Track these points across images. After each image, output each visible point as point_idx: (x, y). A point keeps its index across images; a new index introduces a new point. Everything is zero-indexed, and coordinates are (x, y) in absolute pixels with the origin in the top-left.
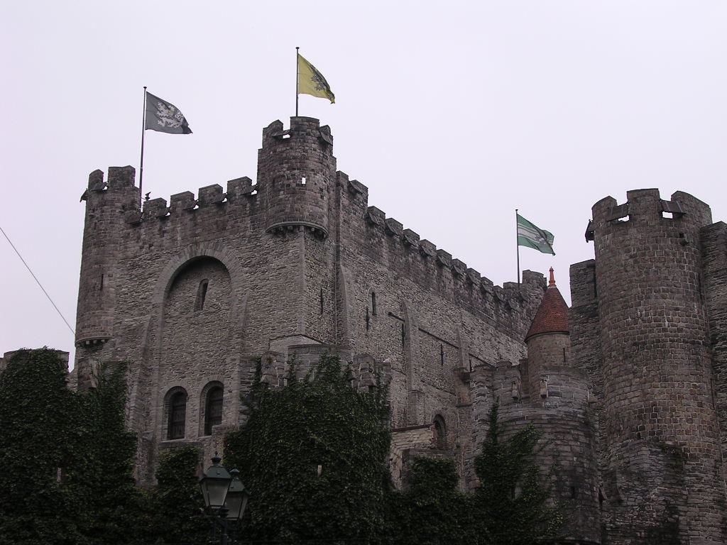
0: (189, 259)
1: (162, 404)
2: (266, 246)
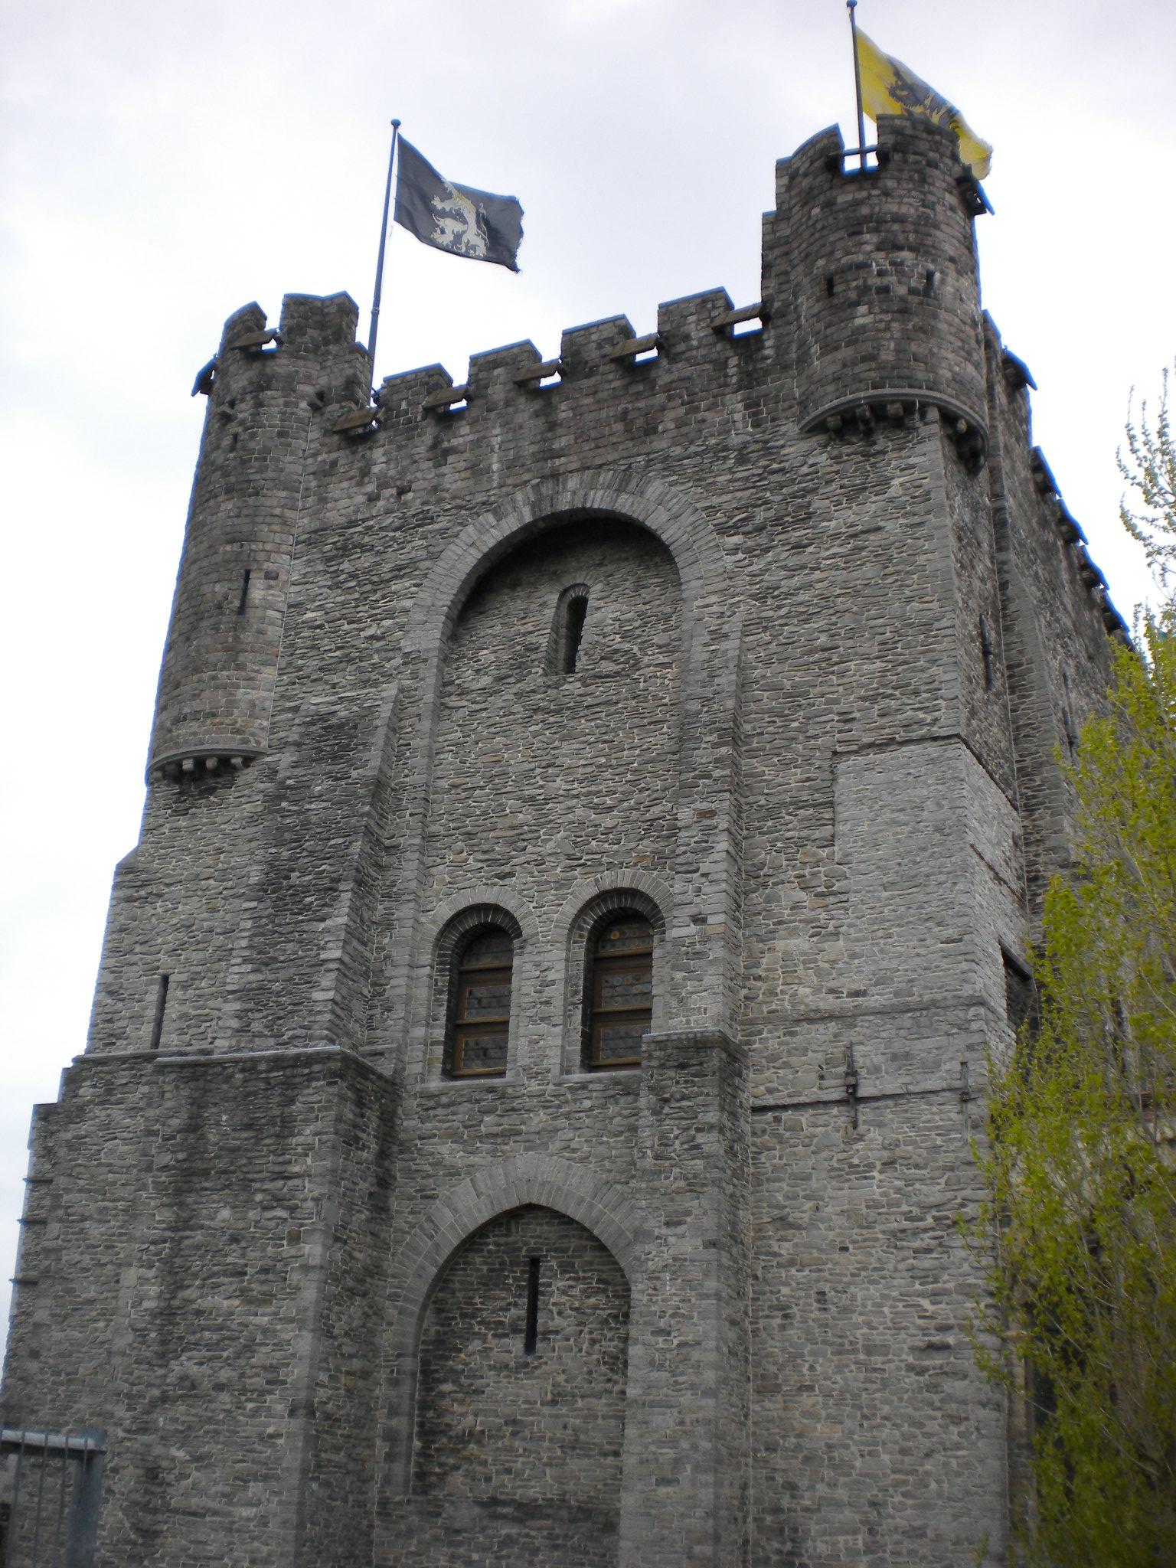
0: (528, 518)
1: (426, 957)
2: (805, 469)
